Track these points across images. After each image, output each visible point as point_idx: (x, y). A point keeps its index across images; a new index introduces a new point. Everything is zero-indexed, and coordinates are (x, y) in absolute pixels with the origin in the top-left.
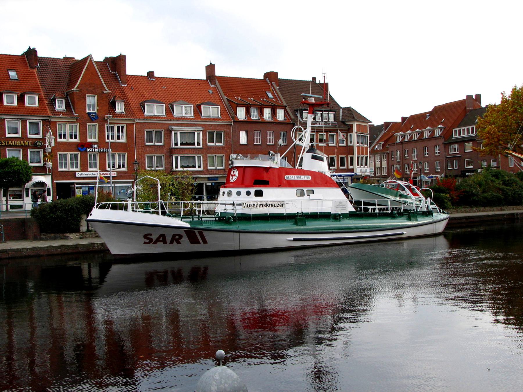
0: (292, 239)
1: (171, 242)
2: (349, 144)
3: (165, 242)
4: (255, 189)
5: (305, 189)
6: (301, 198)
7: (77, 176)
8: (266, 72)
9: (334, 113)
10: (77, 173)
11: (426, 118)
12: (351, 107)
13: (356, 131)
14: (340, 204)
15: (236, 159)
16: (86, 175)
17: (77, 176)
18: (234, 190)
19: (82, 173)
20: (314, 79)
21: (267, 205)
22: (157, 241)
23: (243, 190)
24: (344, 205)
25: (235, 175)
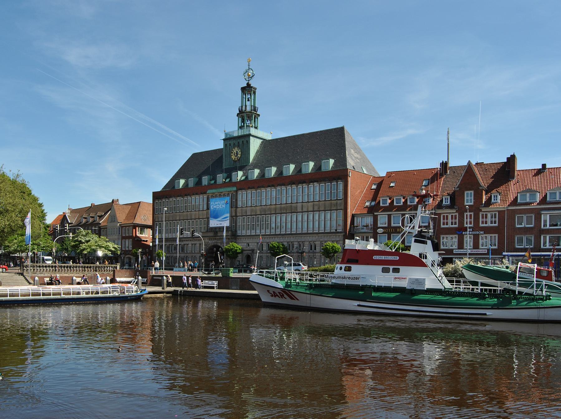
5: (391, 267)
7: (454, 252)
10: (454, 250)
14: (416, 281)
16: (461, 252)
17: (454, 252)
19: (458, 250)
21: (345, 278)
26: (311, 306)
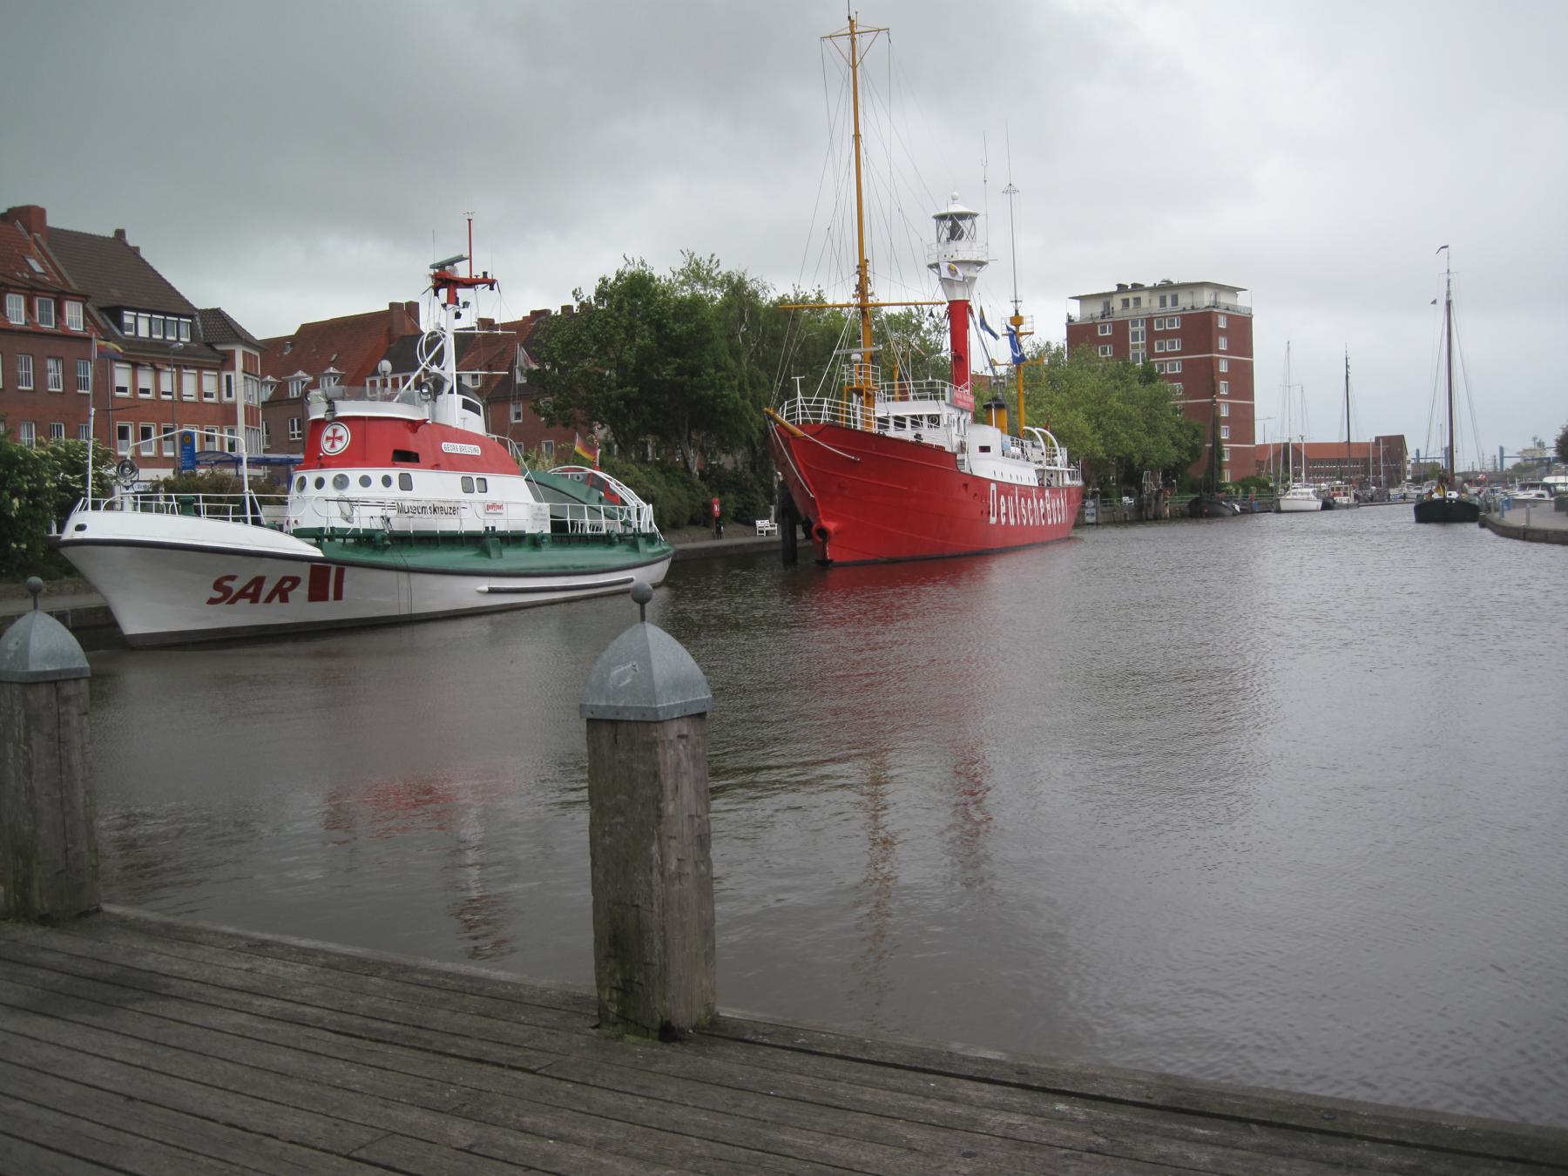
0: (485, 588)
1: (269, 600)
2: (225, 399)
3: (254, 598)
4: (400, 472)
5: (475, 477)
6: (469, 496)
8: (11, 207)
9: (190, 321)
11: (285, 350)
12: (222, 309)
13: (242, 367)
15: (343, 398)
18: (354, 474)
20: (120, 234)
22: (242, 594)
23: (376, 474)
24: (545, 515)
25: (340, 438)
26: (413, 612)
